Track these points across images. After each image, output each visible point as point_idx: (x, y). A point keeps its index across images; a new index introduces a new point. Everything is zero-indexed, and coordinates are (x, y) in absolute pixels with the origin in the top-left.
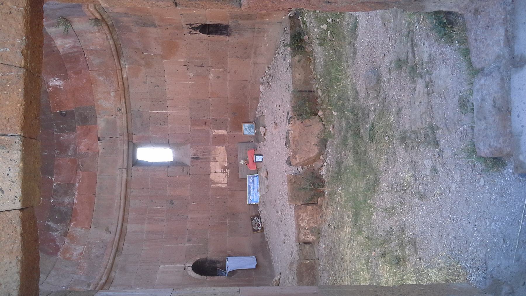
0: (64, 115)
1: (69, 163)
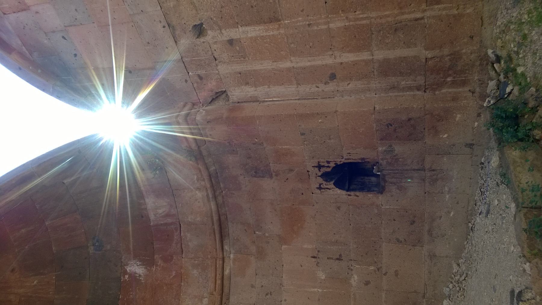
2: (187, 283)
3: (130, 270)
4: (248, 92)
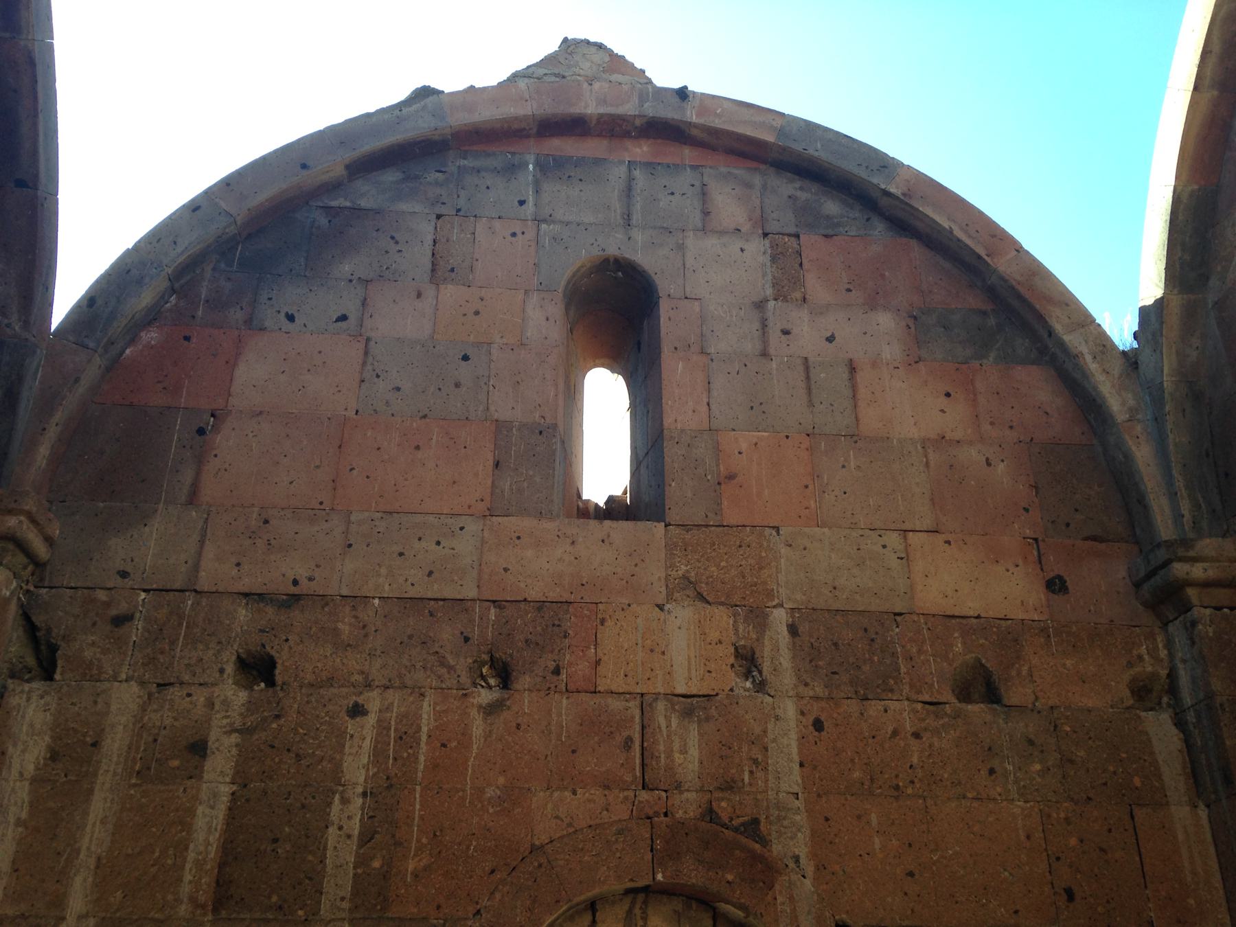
4: (23, 751)
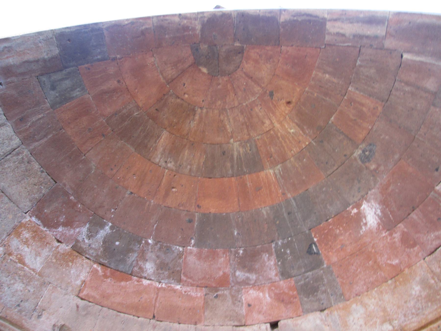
0: (310, 252)
1: (221, 273)
2: (395, 287)
3: (364, 209)
